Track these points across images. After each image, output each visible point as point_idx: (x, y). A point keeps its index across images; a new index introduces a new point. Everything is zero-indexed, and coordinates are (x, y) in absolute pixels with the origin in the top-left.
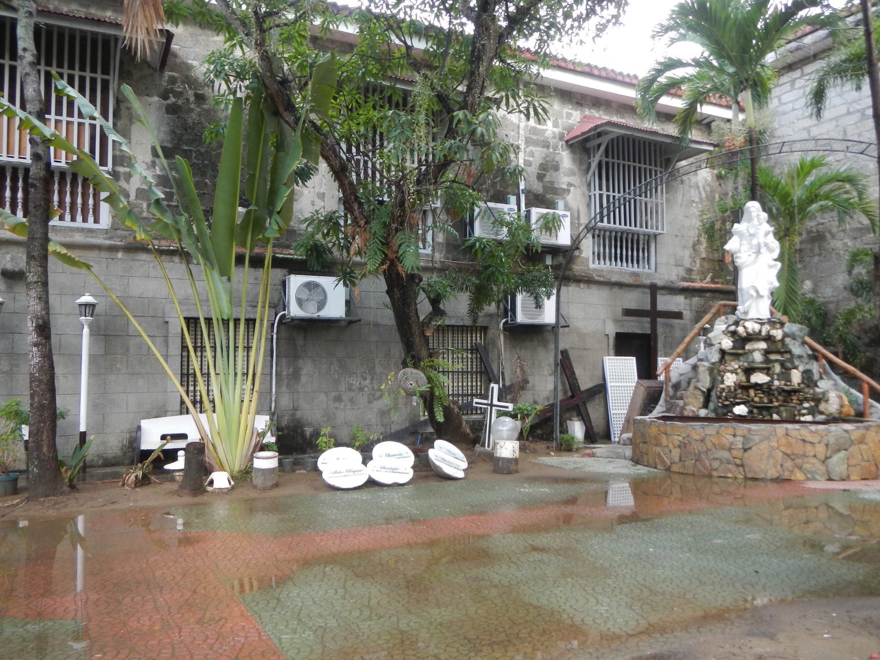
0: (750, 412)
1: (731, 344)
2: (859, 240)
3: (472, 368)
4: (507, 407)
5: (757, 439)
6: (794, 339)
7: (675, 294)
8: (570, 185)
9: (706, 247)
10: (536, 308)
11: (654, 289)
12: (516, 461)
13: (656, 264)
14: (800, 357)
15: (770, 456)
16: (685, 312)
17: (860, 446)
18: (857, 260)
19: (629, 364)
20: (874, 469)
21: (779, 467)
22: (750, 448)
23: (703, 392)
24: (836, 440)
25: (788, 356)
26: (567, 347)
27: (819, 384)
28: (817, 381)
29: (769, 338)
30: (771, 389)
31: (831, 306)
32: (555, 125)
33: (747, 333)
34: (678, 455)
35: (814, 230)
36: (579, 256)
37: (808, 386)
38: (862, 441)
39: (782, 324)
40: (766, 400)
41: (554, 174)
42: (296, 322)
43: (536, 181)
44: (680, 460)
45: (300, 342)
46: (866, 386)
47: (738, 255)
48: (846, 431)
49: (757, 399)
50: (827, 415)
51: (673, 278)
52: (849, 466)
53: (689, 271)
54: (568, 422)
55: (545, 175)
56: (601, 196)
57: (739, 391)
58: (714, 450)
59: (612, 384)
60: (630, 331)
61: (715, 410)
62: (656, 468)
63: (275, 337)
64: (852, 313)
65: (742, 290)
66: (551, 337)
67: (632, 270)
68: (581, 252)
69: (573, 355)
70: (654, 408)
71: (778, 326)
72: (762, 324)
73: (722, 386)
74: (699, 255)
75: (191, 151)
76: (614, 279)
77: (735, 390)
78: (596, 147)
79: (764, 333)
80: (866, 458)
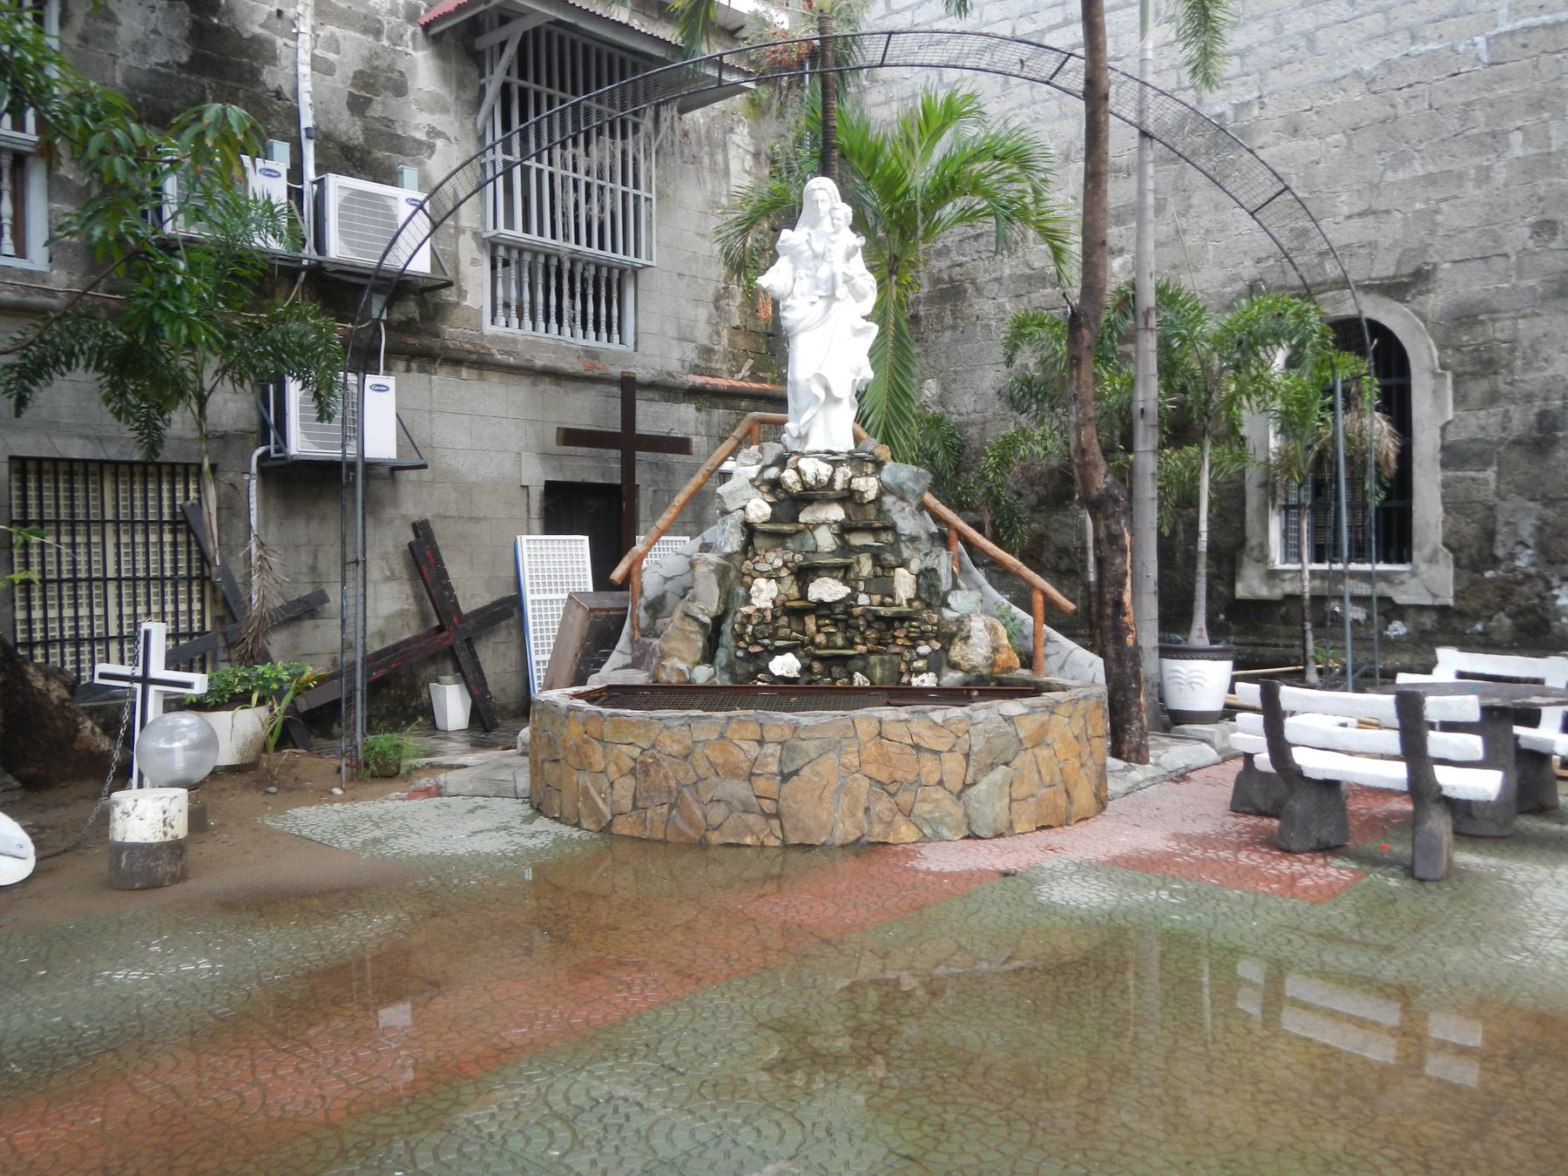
0: (806, 669)
1: (768, 510)
2: (1025, 299)
3: (175, 569)
4: (188, 685)
5: (811, 747)
6: (903, 499)
7: (677, 400)
8: (434, 133)
9: (742, 304)
10: (320, 419)
11: (629, 388)
12: (176, 848)
13: (636, 334)
14: (913, 539)
15: (843, 789)
16: (695, 439)
17: (1036, 750)
18: (1023, 335)
19: (577, 549)
20: (1062, 801)
21: (860, 814)
22: (796, 772)
23: (703, 625)
24: (988, 740)
25: (887, 537)
26: (428, 515)
27: (950, 600)
28: (946, 594)
29: (849, 497)
30: (850, 615)
31: (972, 431)
33: (804, 484)
34: (630, 794)
35: (946, 277)
36: (457, 304)
37: (929, 606)
38: (1039, 741)
39: (879, 465)
40: (840, 641)
41: (395, 102)
43: (346, 114)
44: (635, 807)
46: (1038, 599)
47: (789, 302)
48: (1008, 719)
49: (820, 639)
50: (967, 672)
51: (674, 366)
52: (1011, 800)
53: (707, 352)
54: (433, 685)
57: (784, 621)
58: (714, 779)
59: (536, 596)
60: (579, 480)
61: (729, 668)
62: (578, 825)
64: (1009, 444)
65: (795, 383)
67: (585, 343)
68: (462, 294)
69: (443, 535)
70: (608, 655)
71: (870, 468)
72: (835, 464)
73: (746, 610)
74: (727, 320)
76: (539, 363)
77: (775, 618)
78: (496, 49)
79: (838, 485)
80: (1047, 779)
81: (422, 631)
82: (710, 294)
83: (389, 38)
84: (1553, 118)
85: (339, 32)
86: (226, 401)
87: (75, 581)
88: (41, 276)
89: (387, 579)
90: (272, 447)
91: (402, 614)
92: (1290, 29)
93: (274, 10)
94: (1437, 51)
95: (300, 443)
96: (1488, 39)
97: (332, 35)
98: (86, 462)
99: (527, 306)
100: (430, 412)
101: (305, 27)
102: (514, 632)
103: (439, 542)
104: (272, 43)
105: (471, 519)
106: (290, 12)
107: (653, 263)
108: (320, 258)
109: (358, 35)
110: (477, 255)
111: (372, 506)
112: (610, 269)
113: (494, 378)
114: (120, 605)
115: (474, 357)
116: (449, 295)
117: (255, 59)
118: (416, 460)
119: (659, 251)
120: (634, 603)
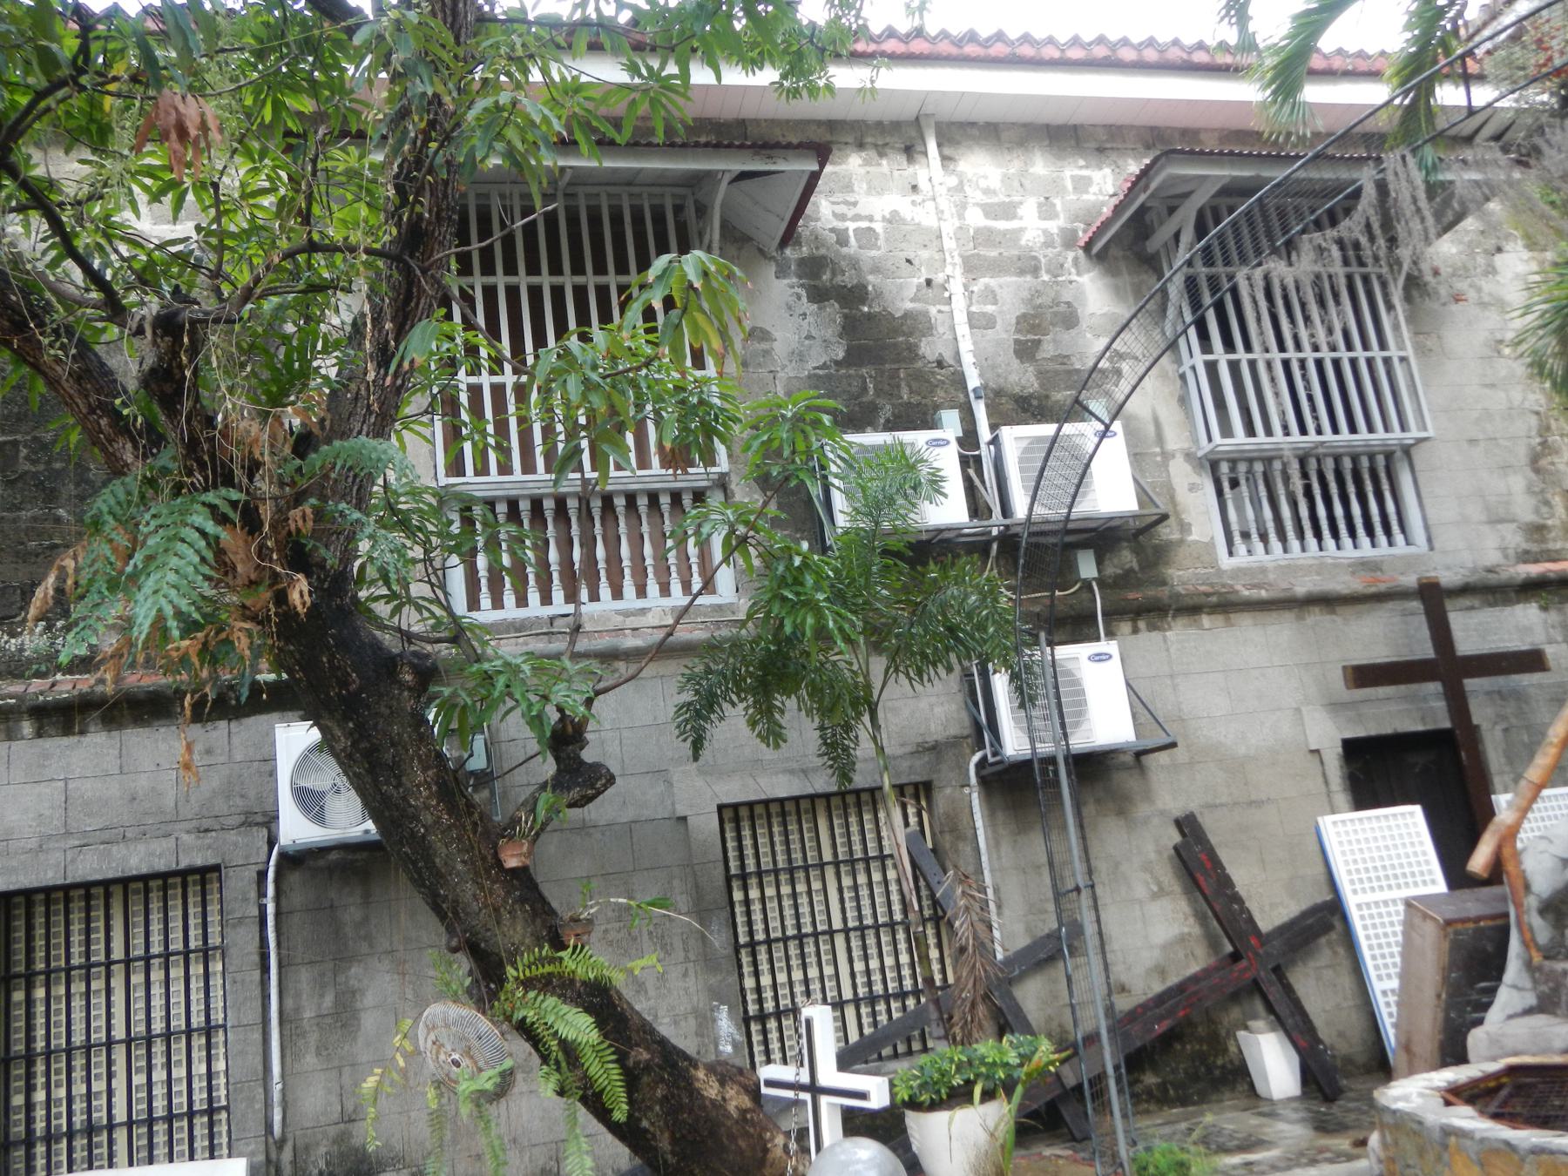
4: (863, 1096)
11: (1433, 598)
13: (1427, 527)
16: (1550, 651)
26: (1193, 806)
32: (1046, 210)
36: (1181, 542)
41: (1066, 336)
42: (334, 856)
43: (1015, 363)
45: (351, 913)
51: (1492, 557)
53: (1537, 531)
54: (1241, 1034)
55: (1037, 344)
56: (1212, 368)
63: (271, 909)
66: (1129, 782)
67: (1357, 554)
68: (1185, 528)
69: (1217, 830)
70: (1492, 992)
75: (15, 443)
76: (1301, 588)
78: (1172, 244)
81: (1212, 961)
82: (1522, 454)
83: (1048, 272)
85: (993, 282)
86: (932, 706)
87: (800, 937)
88: (731, 608)
89: (1155, 896)
90: (988, 750)
91: (1182, 939)
93: (922, 280)
95: (1014, 743)
97: (987, 287)
98: (796, 800)
99: (1271, 526)
100: (1171, 676)
101: (956, 287)
102: (1341, 951)
103: (1213, 840)
104: (926, 314)
105: (1251, 803)
106: (939, 278)
107: (1431, 433)
108: (1007, 522)
109: (1014, 279)
110: (1196, 479)
111: (1121, 806)
112: (1372, 457)
113: (1245, 621)
114: (851, 961)
115: (1214, 599)
116: (1168, 532)
117: (911, 334)
118: (1163, 739)
119: (1434, 419)
120: (1518, 906)
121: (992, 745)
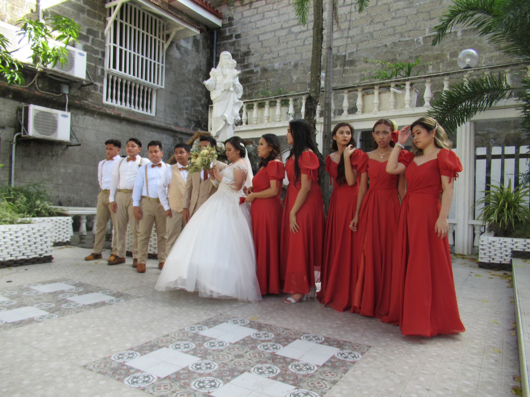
56: (115, 48)
84: (441, 62)
90: (22, 133)
92: (366, 31)
94: (408, 40)
96: (423, 38)
121: (24, 132)
